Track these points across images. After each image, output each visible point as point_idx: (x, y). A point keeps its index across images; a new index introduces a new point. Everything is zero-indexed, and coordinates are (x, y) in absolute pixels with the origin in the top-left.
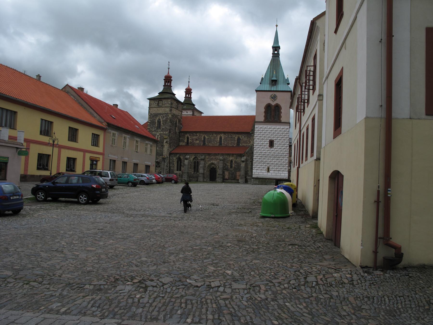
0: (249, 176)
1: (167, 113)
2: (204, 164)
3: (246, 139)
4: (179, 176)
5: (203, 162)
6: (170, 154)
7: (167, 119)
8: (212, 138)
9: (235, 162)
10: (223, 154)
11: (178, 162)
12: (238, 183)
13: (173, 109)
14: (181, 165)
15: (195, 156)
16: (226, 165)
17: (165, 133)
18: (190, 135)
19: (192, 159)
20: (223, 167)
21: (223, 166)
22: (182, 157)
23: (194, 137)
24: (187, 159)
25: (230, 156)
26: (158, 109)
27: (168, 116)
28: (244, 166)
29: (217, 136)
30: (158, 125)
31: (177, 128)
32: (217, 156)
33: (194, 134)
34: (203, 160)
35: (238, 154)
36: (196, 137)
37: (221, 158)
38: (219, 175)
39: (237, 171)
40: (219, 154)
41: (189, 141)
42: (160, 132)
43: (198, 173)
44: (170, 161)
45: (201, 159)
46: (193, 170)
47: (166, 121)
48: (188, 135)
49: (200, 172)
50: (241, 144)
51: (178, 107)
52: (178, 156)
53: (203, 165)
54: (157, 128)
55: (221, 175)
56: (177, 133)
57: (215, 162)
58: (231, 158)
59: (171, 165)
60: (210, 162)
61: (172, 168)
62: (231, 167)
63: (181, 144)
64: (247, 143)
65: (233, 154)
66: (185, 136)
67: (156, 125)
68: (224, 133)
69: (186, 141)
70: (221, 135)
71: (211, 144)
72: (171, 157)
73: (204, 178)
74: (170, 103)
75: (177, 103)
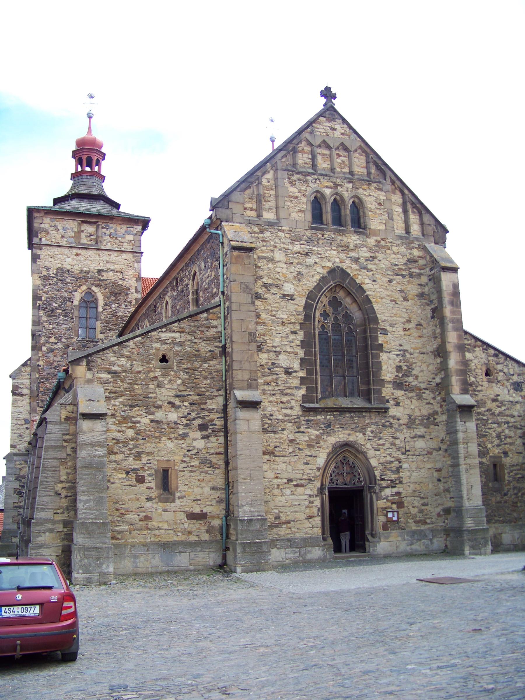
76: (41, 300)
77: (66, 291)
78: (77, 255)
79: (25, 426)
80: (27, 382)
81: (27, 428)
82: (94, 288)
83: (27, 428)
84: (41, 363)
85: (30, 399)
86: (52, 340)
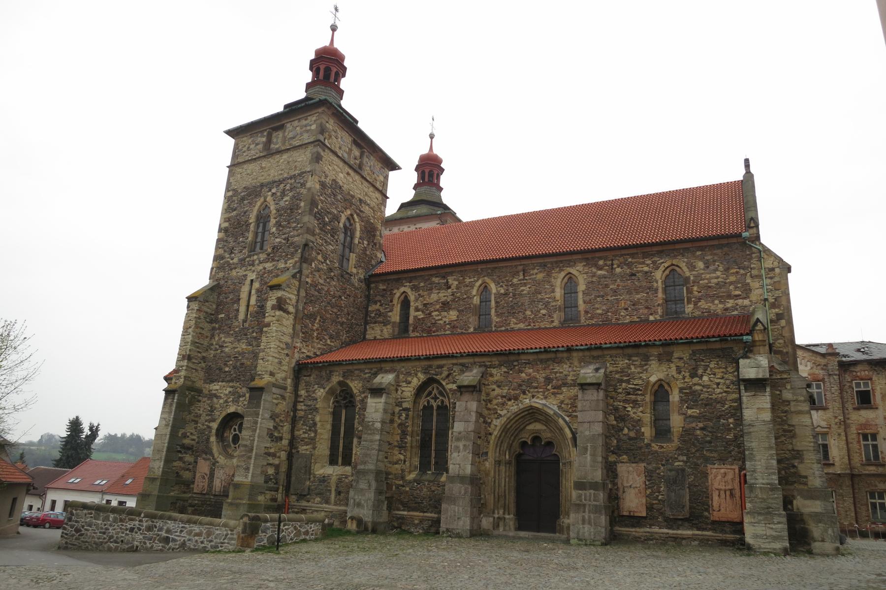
0: (812, 495)
1: (299, 175)
2: (480, 415)
3: (716, 276)
4: (339, 493)
5: (473, 406)
6: (300, 370)
7: (297, 198)
8: (526, 289)
9: (690, 397)
10: (600, 348)
11: (336, 415)
12: (740, 546)
13: (327, 156)
14: (350, 432)
15: (426, 371)
16: (622, 418)
17: (281, 265)
18: (415, 288)
19: (408, 391)
20: (607, 437)
21: (607, 426)
22: (355, 386)
23: (434, 297)
24: (377, 392)
25: (646, 358)
26: (264, 163)
27: (303, 185)
28: (767, 416)
29: (549, 275)
30: (256, 234)
31: (353, 256)
32: (560, 362)
33: (436, 280)
34: (472, 389)
35: (704, 340)
36: (444, 295)
37: (588, 373)
38: (580, 486)
39: (707, 460)
40: (569, 350)
41: (412, 313)
42: (261, 267)
43: (443, 478)
44: (295, 409)
45: (462, 389)
46: (416, 461)
47: (292, 208)
48: (406, 288)
49: (452, 468)
50: (689, 308)
51: (360, 166)
52: (336, 379)
53: (471, 427)
54: (252, 250)
55: (594, 486)
56: (355, 281)
57: (550, 404)
58: (656, 373)
59: (299, 433)
60: (514, 407)
61: (303, 449)
62: (662, 432)
63: (375, 331)
64: (730, 296)
65: (667, 344)
66: (392, 295)
67: (250, 236)
68: (589, 256)
69: (395, 316)
70: (573, 271)
71: (520, 321)
72: (302, 385)
73: (479, 507)
74: (314, 127)
75: (355, 142)
76: (317, 208)
77: (336, 208)
78: (348, 174)
79: (286, 352)
80: (294, 298)
81: (287, 355)
82: (355, 216)
83: (287, 355)
84: (309, 280)
85: (295, 317)
86: (320, 257)
